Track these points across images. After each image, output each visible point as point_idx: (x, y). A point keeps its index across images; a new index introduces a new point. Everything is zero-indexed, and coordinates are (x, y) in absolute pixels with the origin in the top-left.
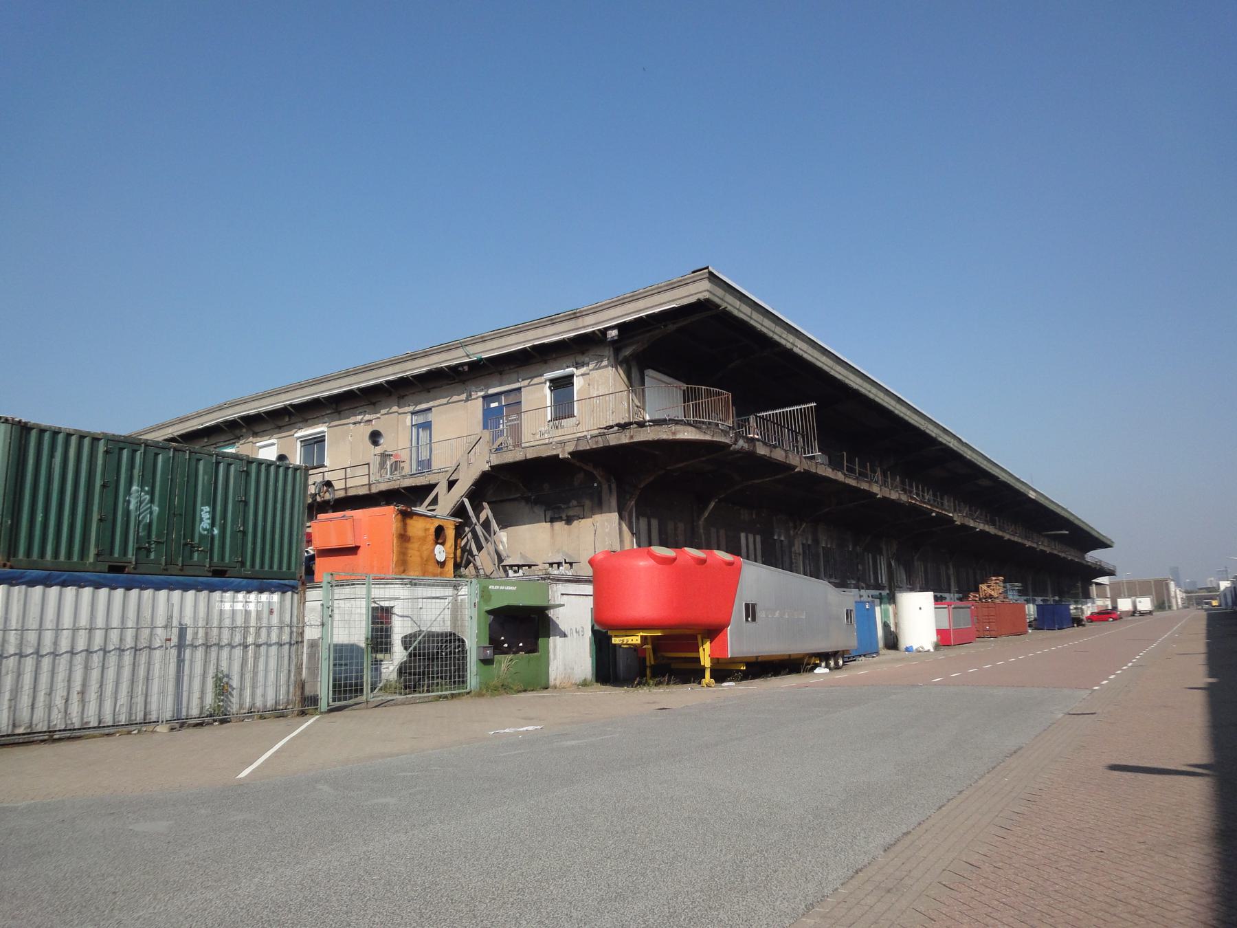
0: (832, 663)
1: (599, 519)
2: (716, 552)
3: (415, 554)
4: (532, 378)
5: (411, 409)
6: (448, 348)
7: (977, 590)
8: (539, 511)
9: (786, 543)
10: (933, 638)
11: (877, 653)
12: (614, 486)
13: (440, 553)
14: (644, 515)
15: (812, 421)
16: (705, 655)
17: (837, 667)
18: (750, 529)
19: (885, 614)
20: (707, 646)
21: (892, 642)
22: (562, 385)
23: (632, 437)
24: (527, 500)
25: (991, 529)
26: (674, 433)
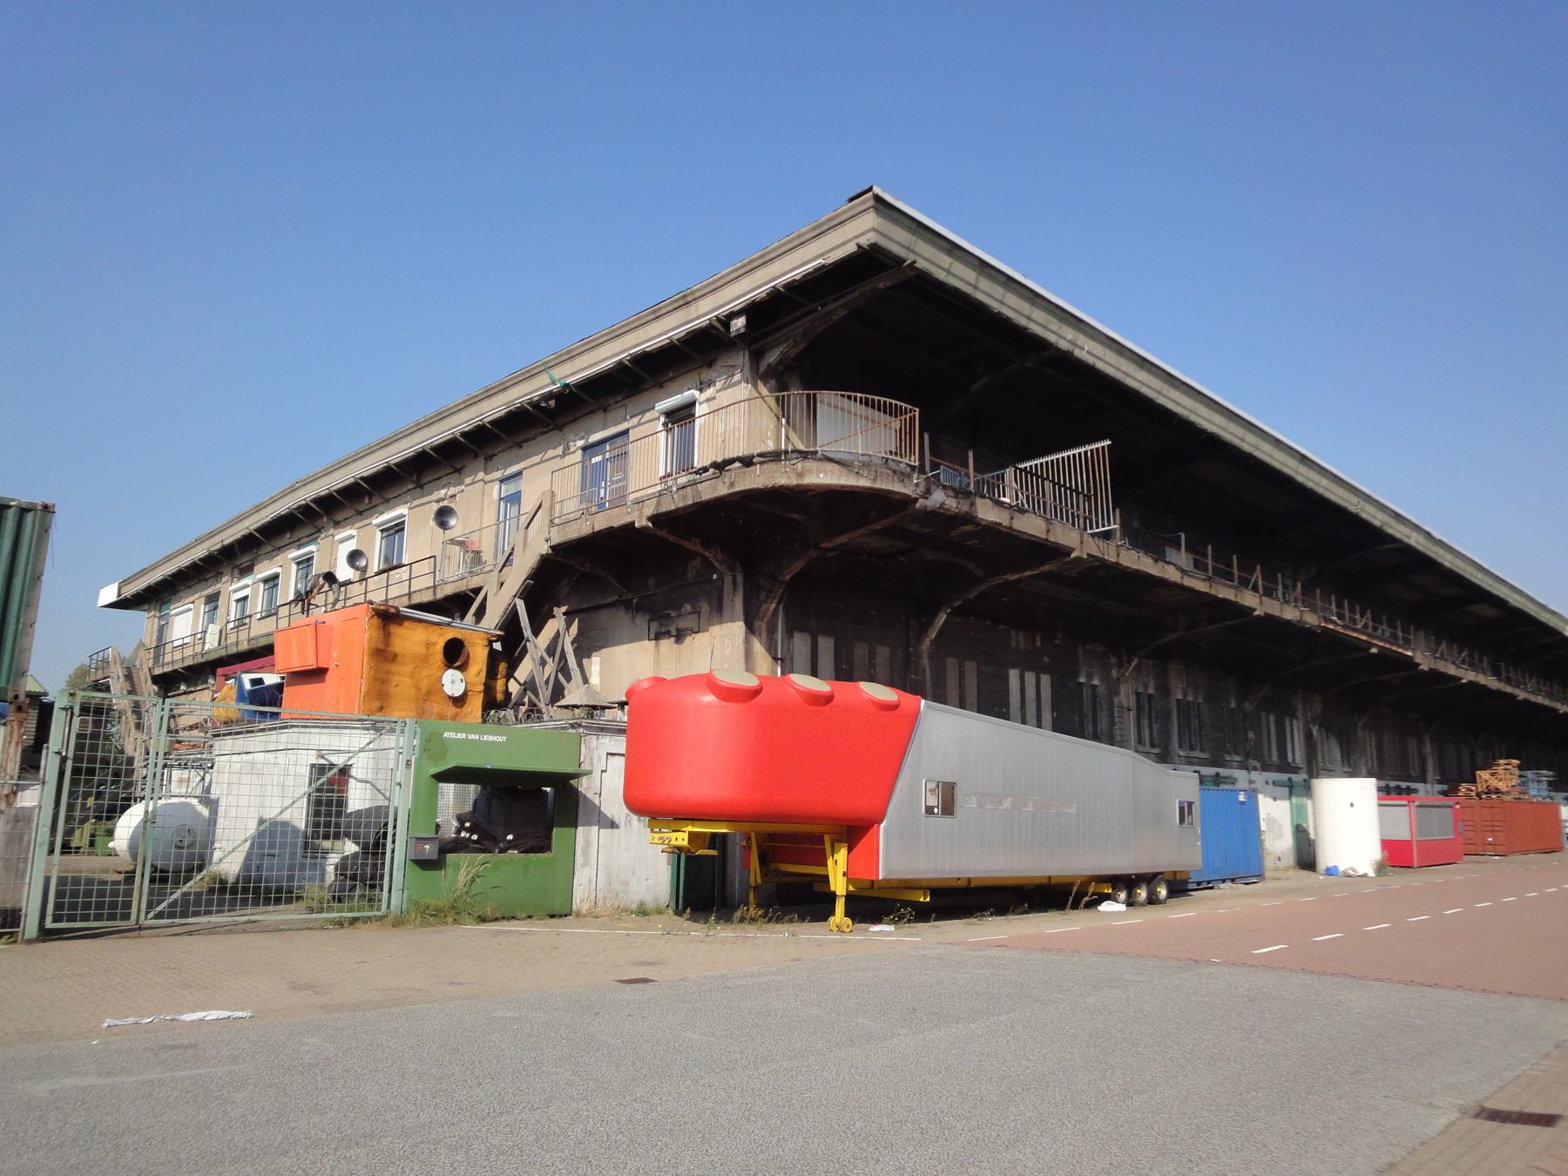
0: (1142, 894)
1: (716, 630)
3: (402, 681)
4: (644, 412)
5: (498, 474)
6: (530, 375)
7: (1474, 781)
8: (641, 621)
9: (1102, 690)
10: (1376, 854)
11: (1260, 876)
12: (740, 578)
13: (453, 682)
14: (800, 630)
15: (1105, 475)
16: (838, 872)
17: (1152, 900)
18: (1029, 662)
19: (1298, 812)
20: (842, 855)
21: (1306, 858)
22: (681, 416)
23: (732, 484)
24: (627, 605)
25: (1492, 683)
26: (800, 475)
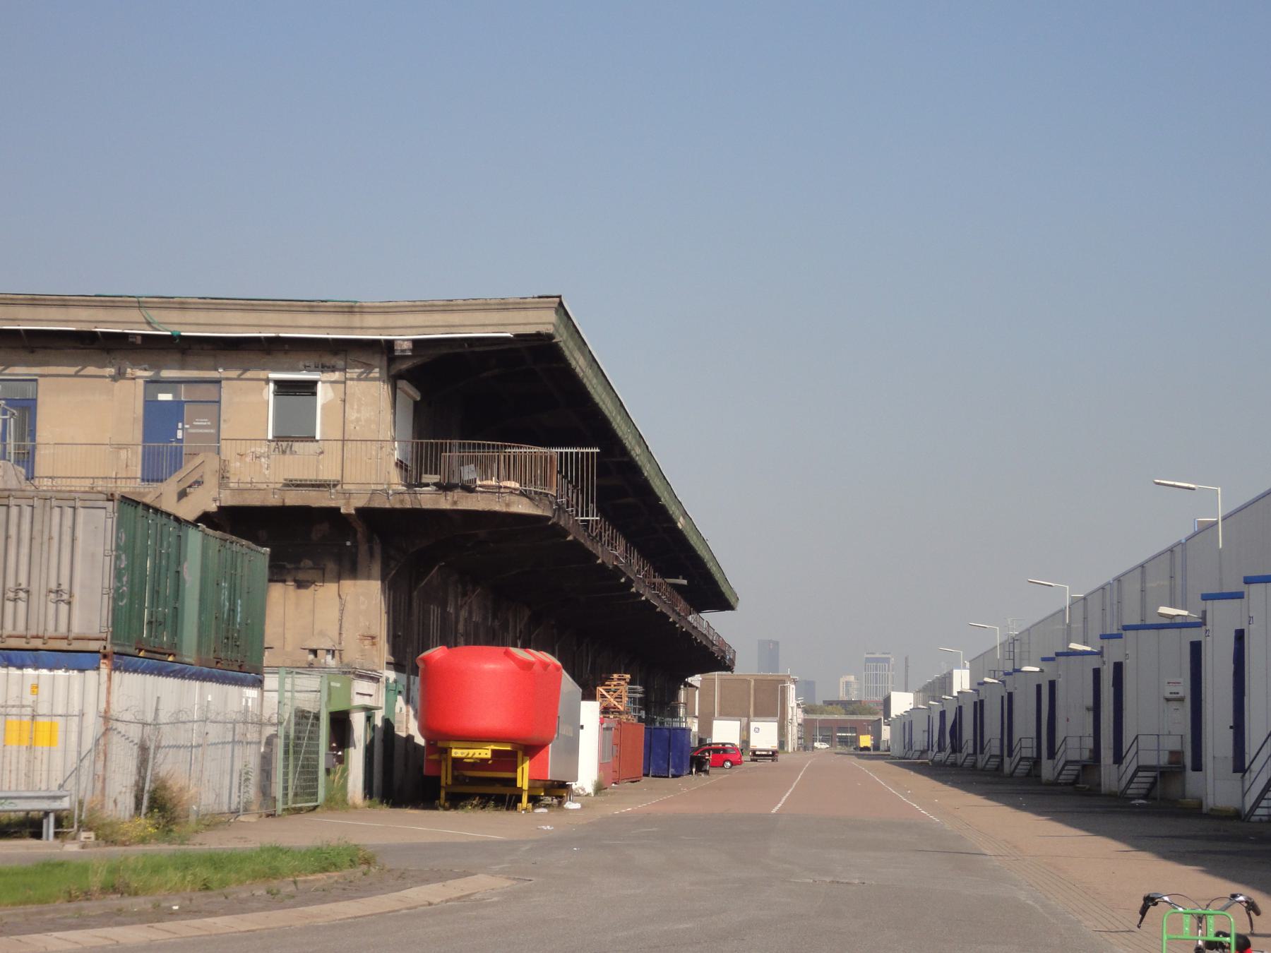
1: (348, 585)
2: (513, 650)
12: (377, 550)
20: (526, 765)
23: (455, 503)
26: (508, 505)
